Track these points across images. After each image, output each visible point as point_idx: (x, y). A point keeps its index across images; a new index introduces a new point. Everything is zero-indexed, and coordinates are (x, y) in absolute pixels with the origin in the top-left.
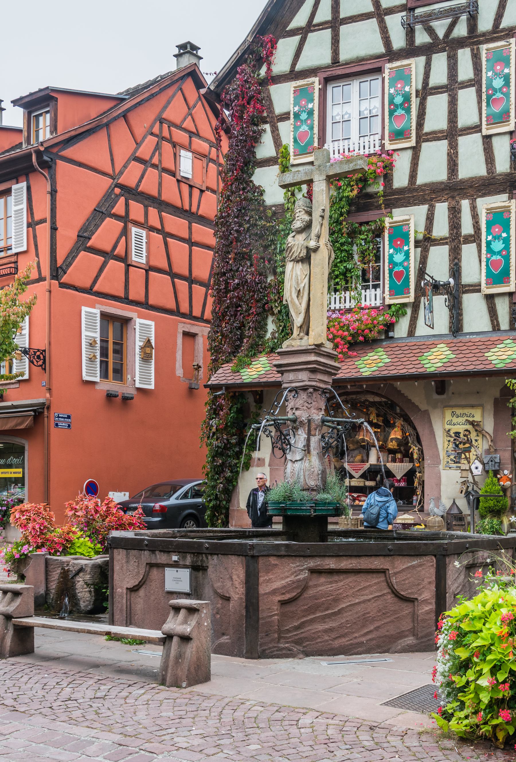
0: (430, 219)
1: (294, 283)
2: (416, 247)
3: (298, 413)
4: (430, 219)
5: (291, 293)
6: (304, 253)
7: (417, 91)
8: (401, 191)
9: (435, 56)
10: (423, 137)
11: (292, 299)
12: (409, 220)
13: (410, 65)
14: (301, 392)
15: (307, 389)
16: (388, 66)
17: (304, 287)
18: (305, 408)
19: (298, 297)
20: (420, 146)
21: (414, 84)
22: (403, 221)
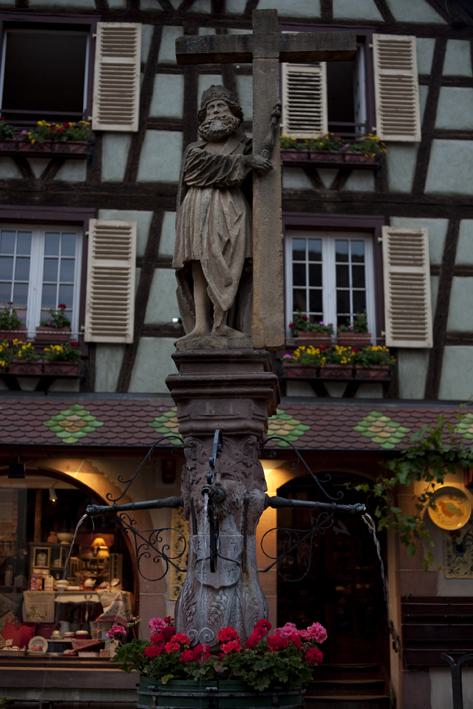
0: (155, 231)
1: (218, 228)
2: (138, 265)
3: (226, 484)
4: (155, 231)
5: (210, 244)
6: (238, 175)
7: (142, 65)
8: (112, 186)
9: (166, 29)
10: (149, 123)
11: (213, 256)
12: (129, 228)
13: (133, 29)
14: (231, 443)
15: (248, 435)
16: (101, 25)
17: (238, 236)
18: (240, 475)
19: (224, 253)
20: (144, 134)
21: (138, 52)
22: (120, 228)
